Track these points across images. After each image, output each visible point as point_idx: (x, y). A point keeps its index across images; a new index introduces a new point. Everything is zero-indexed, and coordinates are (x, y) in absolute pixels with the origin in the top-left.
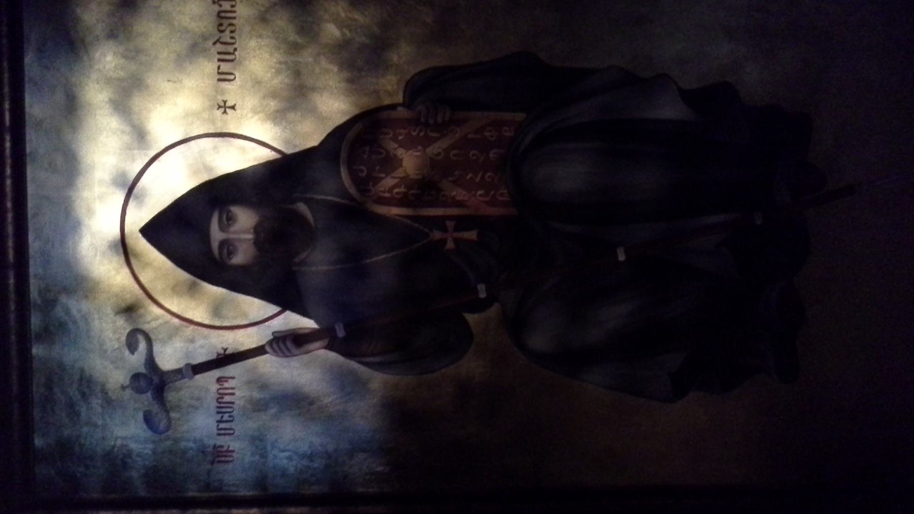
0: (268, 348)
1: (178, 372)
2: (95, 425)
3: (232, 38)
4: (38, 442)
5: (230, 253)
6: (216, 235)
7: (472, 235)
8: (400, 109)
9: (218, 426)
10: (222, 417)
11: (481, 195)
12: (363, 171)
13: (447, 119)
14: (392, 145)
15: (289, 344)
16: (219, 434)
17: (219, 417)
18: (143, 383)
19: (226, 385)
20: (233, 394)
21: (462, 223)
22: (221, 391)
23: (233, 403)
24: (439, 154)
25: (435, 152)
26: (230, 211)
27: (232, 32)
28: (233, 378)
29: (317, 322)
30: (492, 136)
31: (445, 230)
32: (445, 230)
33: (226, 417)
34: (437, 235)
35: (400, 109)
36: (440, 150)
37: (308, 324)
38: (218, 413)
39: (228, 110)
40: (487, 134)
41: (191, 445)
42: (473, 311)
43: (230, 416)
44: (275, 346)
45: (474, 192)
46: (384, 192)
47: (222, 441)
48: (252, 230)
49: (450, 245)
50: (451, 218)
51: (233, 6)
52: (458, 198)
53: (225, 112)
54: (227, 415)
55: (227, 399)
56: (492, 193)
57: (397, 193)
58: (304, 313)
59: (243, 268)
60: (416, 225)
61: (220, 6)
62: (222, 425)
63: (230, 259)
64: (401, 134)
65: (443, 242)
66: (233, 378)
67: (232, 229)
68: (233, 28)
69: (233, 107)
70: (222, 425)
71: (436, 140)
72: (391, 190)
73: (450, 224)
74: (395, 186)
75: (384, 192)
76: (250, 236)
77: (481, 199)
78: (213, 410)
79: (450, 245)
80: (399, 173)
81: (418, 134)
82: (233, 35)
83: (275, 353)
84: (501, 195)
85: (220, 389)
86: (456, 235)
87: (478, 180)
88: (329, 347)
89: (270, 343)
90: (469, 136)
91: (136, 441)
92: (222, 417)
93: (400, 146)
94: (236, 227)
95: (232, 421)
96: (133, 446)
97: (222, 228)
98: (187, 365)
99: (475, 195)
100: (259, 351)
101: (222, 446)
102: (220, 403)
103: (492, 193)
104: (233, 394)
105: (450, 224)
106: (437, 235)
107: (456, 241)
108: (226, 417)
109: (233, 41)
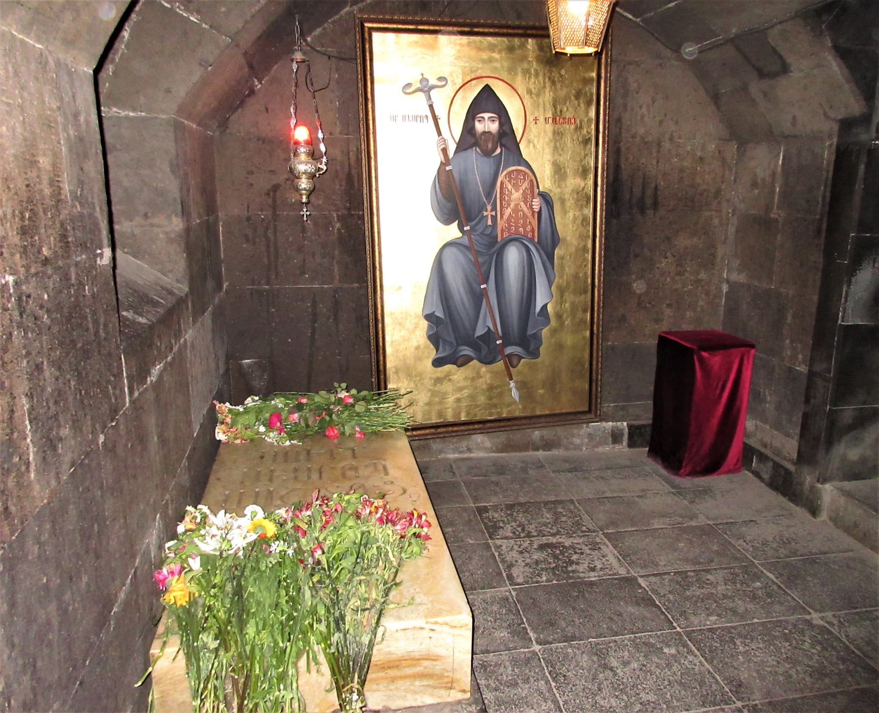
5: (479, 121)
6: (486, 115)
7: (490, 223)
15: (443, 146)
18: (424, 83)
19: (425, 119)
21: (494, 218)
31: (492, 211)
32: (492, 211)
33: (411, 119)
34: (489, 208)
42: (458, 225)
49: (485, 214)
50: (496, 213)
55: (419, 119)
58: (456, 152)
59: (473, 127)
65: (486, 211)
73: (493, 213)
79: (485, 214)
80: (513, 191)
86: (490, 216)
89: (443, 138)
97: (489, 118)
100: (439, 133)
106: (489, 208)
107: (487, 216)
108: (411, 119)
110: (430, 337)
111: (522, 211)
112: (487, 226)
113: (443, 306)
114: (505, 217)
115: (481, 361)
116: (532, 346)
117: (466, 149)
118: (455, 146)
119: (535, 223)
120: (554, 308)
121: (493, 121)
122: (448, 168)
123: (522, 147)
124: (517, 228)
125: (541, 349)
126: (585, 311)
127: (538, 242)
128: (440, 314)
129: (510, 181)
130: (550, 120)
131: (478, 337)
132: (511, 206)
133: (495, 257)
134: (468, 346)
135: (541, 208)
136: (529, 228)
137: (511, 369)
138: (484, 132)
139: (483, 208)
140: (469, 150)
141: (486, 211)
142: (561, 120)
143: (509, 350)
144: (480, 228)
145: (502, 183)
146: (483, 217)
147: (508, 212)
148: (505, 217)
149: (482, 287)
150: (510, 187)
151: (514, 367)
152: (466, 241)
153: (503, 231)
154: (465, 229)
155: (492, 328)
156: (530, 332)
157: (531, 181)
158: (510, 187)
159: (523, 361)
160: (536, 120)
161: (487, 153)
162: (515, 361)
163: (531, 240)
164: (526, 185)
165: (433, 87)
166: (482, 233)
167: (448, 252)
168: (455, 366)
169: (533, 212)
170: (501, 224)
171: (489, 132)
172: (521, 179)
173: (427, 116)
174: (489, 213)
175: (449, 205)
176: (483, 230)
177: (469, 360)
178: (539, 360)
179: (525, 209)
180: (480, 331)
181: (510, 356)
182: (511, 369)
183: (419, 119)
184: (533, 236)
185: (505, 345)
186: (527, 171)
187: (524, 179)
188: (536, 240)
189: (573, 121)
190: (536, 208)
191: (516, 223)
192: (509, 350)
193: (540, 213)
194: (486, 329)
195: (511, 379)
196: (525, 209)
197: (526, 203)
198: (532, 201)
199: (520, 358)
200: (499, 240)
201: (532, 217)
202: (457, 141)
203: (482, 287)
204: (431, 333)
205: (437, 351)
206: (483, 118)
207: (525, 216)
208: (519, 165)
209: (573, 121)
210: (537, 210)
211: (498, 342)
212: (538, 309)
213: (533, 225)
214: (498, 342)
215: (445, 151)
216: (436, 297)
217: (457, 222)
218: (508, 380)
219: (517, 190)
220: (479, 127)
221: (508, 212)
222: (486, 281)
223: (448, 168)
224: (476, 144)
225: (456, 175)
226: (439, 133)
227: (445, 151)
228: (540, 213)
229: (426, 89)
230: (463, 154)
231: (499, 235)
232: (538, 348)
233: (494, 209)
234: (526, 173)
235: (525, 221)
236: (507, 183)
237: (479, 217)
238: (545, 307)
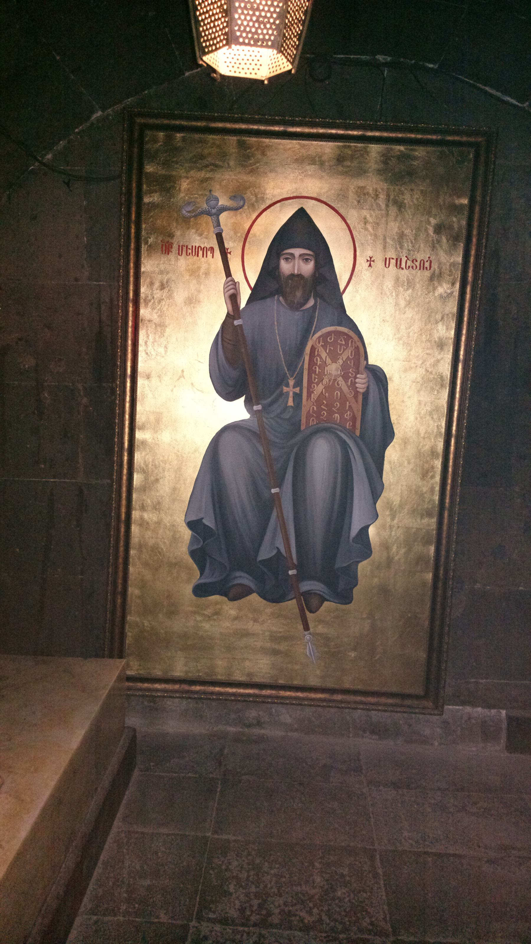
0: (229, 278)
1: (219, 225)
3: (409, 267)
4: (179, 135)
5: (287, 259)
6: (297, 252)
7: (291, 403)
8: (365, 362)
10: (190, 249)
11: (313, 408)
12: (331, 339)
13: (358, 389)
15: (232, 291)
16: (179, 246)
18: (212, 203)
19: (209, 253)
20: (203, 256)
21: (298, 397)
22: (205, 249)
23: (198, 256)
24: (338, 384)
25: (340, 383)
26: (311, 260)
27: (412, 267)
28: (213, 257)
30: (347, 416)
31: (294, 387)
32: (294, 387)
34: (291, 382)
35: (365, 362)
36: (340, 385)
37: (243, 304)
38: (192, 246)
39: (369, 262)
40: (349, 413)
42: (246, 401)
43: (190, 254)
44: (231, 283)
45: (315, 404)
50: (301, 390)
51: (427, 268)
52: (312, 395)
53: (368, 261)
54: (190, 251)
55: (201, 253)
56: (315, 415)
57: (317, 360)
59: (278, 266)
61: (427, 261)
62: (185, 249)
64: (351, 363)
65: (287, 385)
66: (213, 257)
67: (301, 262)
68: (415, 267)
69: (370, 265)
70: (185, 249)
71: (346, 382)
72: (319, 355)
73: (297, 390)
74: (321, 358)
76: (296, 272)
77: (311, 408)
79: (285, 389)
80: (329, 361)
81: (350, 372)
82: (411, 268)
84: (313, 420)
85: (207, 248)
86: (291, 394)
87: (322, 407)
88: (228, 315)
89: (233, 280)
90: (348, 403)
92: (190, 249)
93: (344, 362)
94: (302, 263)
95: (187, 255)
97: (301, 255)
99: (313, 405)
100: (228, 273)
101: (172, 248)
103: (315, 415)
104: (203, 256)
105: (297, 390)
106: (291, 382)
110: (193, 554)
111: (340, 389)
112: (286, 407)
113: (215, 514)
114: (314, 397)
115: (263, 596)
116: (341, 585)
117: (264, 298)
118: (250, 292)
119: (357, 407)
120: (378, 534)
121: (307, 260)
122: (236, 323)
123: (346, 298)
124: (331, 413)
125: (355, 591)
126: (427, 543)
127: (362, 436)
128: (209, 522)
129: (324, 347)
130: (393, 262)
131: (263, 562)
132: (324, 382)
133: (295, 451)
134: (247, 573)
135: (368, 388)
136: (347, 415)
137: (308, 613)
138: (292, 276)
139: (282, 381)
140: (268, 300)
141: (287, 385)
142: (409, 263)
143: (306, 586)
144: (277, 409)
145: (313, 349)
146: (281, 394)
147: (319, 389)
148: (314, 397)
149: (273, 491)
150: (324, 355)
151: (311, 612)
152: (255, 426)
153: (308, 416)
154: (256, 408)
155: (283, 550)
156: (340, 563)
157: (357, 348)
158: (324, 355)
159: (326, 603)
160: (370, 261)
161: (295, 307)
162: (314, 601)
163: (351, 433)
164: (347, 354)
165: (224, 209)
166: (278, 416)
167: (226, 436)
168: (225, 599)
169: (357, 393)
170: (307, 405)
171: (300, 276)
172: (341, 345)
173: (212, 249)
174: (290, 390)
175: (235, 374)
176: (281, 413)
177: (246, 592)
178: (351, 606)
179: (345, 388)
180: (265, 553)
181: (307, 595)
182: (308, 613)
183: (201, 253)
184: (354, 426)
185: (302, 577)
186: (352, 334)
187: (347, 345)
188: (358, 433)
189: (427, 265)
190: (361, 386)
191: (330, 406)
192: (306, 586)
193: (366, 395)
194: (275, 552)
195: (306, 628)
196: (345, 388)
197: (345, 377)
198: (356, 378)
199: (323, 600)
200: (303, 427)
201: (354, 400)
202: (252, 285)
203: (273, 491)
204: (195, 547)
205: (201, 574)
206: (292, 255)
207: (343, 399)
208: (340, 324)
209: (427, 265)
210: (362, 391)
211: (291, 572)
212: (354, 531)
213: (356, 412)
214: (291, 572)
215: (234, 299)
216: (206, 498)
217: (244, 398)
218: (301, 627)
219: (334, 360)
220: (286, 267)
221: (319, 389)
222: (279, 485)
223: (236, 323)
224: (280, 291)
225: (247, 332)
226: (228, 273)
227: (234, 299)
228: (366, 395)
229: (214, 211)
230: (257, 305)
231: (304, 420)
232: (351, 589)
233: (299, 383)
234: (349, 337)
235: (343, 404)
236: (321, 350)
237: (278, 392)
238: (364, 530)
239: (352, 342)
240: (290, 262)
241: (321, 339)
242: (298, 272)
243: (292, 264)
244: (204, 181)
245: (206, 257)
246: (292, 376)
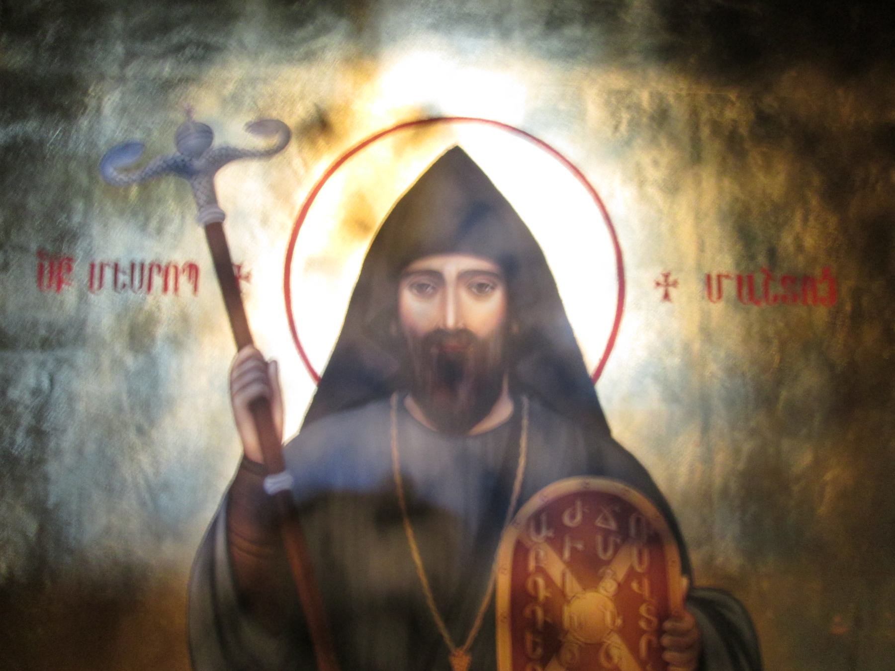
0: (247, 351)
1: (212, 199)
2: (124, 64)
5: (421, 289)
8: (684, 582)
9: (108, 265)
10: (124, 273)
12: (573, 517)
14: (620, 569)
15: (254, 390)
16: (92, 266)
17: (124, 264)
18: (193, 142)
19: (183, 279)
20: (165, 288)
22: (172, 272)
24: (609, 657)
25: (615, 652)
26: (493, 288)
29: (295, 441)
36: (616, 660)
38: (133, 266)
41: (77, 219)
44: (250, 364)
46: (537, 558)
47: (80, 270)
48: (461, 325)
55: (158, 280)
57: (535, 584)
59: (394, 310)
60: (477, 623)
62: (108, 274)
63: (411, 286)
64: (640, 584)
69: (666, 296)
70: (108, 274)
71: (634, 649)
72: (540, 570)
74: (549, 581)
75: (537, 558)
76: (451, 322)
78: (138, 257)
80: (572, 585)
83: (239, 365)
85: (176, 268)
88: (246, 463)
89: (258, 356)
91: (91, 128)
93: (619, 585)
94: (466, 297)
96: (84, 123)
97: (464, 277)
98: (223, 216)
100: (243, 337)
101: (70, 269)
102: (151, 270)
104: (165, 288)
108: (122, 278)
109: (771, 297)
239: (638, 521)
240: (431, 296)
241: (544, 518)
242: (457, 322)
243: (437, 299)
244: (167, 86)
245: (176, 289)
246: (460, 643)
